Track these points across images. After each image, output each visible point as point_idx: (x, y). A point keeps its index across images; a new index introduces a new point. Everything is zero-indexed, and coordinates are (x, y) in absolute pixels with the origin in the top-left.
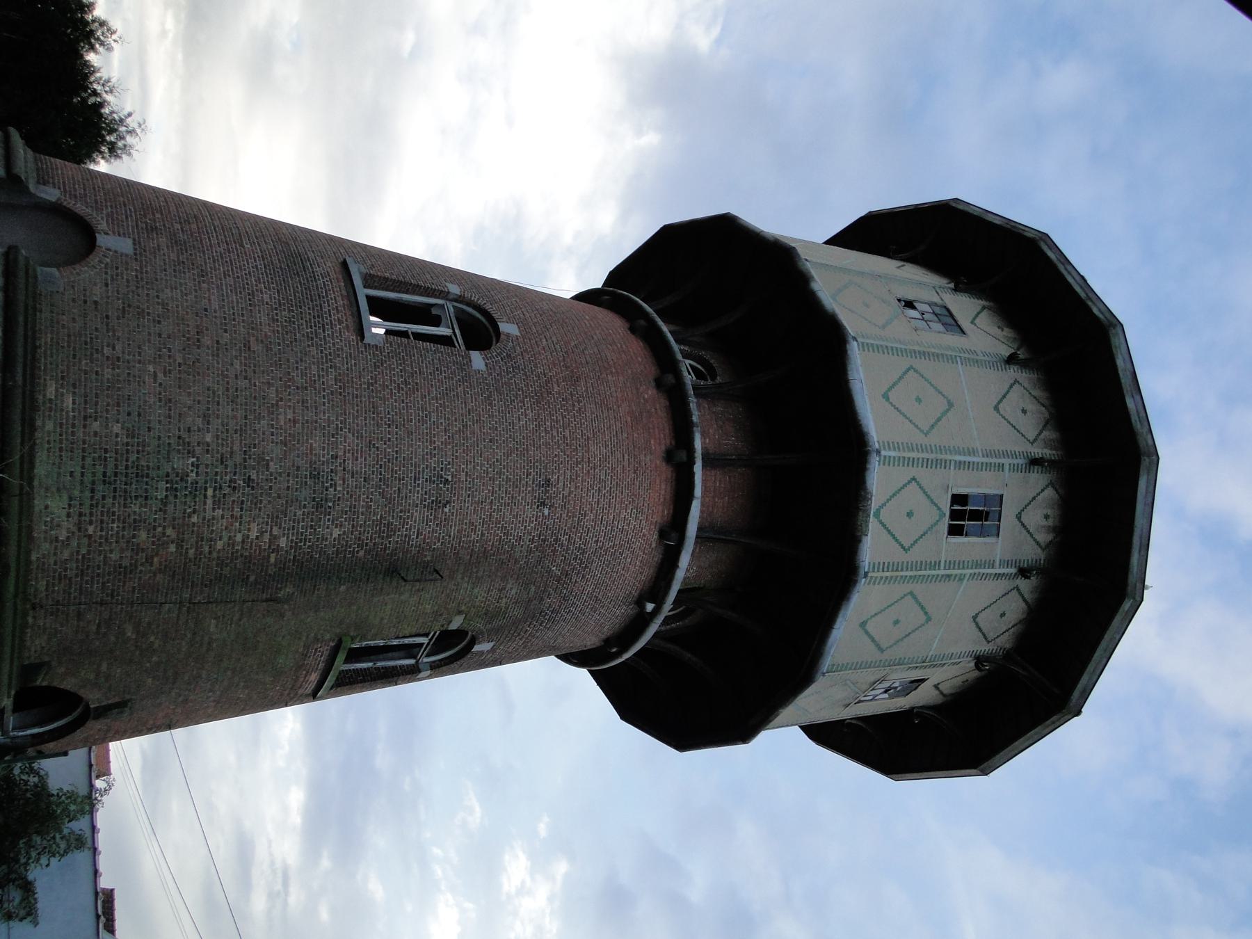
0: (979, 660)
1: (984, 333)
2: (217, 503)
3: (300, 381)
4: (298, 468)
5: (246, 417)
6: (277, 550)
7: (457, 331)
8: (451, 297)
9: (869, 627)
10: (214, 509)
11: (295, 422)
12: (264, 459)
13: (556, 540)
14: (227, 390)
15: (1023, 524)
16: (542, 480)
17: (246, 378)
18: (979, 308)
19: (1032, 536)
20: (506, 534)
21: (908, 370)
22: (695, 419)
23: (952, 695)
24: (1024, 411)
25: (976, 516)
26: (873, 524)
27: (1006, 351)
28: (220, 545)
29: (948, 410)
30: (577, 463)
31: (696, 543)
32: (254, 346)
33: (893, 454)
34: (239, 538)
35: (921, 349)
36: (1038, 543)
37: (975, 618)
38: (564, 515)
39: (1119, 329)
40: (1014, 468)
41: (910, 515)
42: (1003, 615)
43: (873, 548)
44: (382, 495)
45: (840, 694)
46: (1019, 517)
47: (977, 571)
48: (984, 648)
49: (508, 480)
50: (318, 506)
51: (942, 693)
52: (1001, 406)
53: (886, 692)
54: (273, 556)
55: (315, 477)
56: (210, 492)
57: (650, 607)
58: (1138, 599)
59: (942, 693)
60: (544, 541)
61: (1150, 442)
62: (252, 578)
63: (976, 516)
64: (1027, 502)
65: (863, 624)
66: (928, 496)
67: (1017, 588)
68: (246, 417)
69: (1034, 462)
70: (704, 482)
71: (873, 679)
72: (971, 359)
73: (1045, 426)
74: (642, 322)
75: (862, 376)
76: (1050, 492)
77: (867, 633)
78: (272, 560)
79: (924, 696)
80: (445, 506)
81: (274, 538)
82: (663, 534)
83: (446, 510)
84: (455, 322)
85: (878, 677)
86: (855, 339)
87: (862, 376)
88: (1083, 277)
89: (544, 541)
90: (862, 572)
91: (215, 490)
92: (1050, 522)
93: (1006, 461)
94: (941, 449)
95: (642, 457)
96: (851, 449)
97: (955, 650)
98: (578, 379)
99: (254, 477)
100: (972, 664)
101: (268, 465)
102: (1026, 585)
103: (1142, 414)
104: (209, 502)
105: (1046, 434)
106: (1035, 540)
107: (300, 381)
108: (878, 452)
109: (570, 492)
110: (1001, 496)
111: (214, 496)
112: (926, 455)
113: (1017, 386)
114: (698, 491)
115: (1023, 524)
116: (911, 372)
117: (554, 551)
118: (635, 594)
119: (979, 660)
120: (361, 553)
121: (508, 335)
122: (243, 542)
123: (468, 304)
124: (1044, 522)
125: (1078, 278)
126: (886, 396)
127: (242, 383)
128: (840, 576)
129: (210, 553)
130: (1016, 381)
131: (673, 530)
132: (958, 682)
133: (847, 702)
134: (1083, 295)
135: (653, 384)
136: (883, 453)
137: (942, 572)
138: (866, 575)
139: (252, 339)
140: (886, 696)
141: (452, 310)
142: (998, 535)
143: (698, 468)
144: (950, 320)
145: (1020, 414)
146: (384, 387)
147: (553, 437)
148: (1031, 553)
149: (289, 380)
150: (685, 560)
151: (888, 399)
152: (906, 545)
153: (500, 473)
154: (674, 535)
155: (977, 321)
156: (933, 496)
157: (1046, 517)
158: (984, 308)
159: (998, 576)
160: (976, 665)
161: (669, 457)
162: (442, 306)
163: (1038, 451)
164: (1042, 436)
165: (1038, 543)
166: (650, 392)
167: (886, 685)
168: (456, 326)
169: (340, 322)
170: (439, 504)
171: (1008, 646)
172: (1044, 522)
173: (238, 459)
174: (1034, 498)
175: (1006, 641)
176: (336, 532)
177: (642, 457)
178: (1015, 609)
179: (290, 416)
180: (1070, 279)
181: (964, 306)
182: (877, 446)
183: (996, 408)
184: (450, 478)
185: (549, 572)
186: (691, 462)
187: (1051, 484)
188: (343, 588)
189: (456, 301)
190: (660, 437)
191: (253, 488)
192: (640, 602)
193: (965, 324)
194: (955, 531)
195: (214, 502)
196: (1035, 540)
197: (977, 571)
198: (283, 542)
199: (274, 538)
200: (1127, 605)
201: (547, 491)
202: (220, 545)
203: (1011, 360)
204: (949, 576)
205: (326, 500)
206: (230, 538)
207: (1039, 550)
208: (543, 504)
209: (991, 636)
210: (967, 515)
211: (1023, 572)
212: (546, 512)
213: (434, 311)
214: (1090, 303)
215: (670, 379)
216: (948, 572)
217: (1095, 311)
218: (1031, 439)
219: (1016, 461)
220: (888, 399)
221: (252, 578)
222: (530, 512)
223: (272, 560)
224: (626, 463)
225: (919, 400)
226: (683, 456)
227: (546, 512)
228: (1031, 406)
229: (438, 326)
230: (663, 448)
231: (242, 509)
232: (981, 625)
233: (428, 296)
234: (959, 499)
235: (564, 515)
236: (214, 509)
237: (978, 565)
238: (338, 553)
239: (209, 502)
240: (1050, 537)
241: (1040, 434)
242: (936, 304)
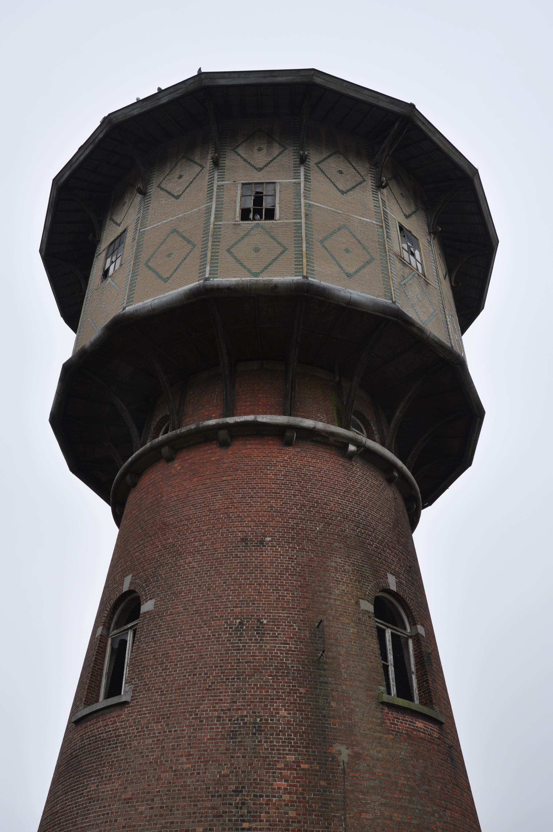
0: (380, 186)
1: (128, 218)
2: (255, 818)
3: (157, 753)
4: (227, 749)
5: (184, 798)
6: (298, 763)
7: (129, 626)
8: (105, 633)
9: (351, 270)
10: (260, 821)
11: (189, 755)
12: (219, 780)
13: (293, 529)
14: (161, 815)
15: (266, 166)
16: (241, 545)
17: (153, 800)
18: (111, 222)
19: (275, 158)
20: (287, 569)
21: (150, 268)
22: (193, 427)
23: (416, 205)
24: (180, 177)
25: (258, 199)
26: (264, 278)
27: (139, 197)
28: (292, 814)
29: (178, 232)
30: (229, 517)
31: (297, 416)
32: (129, 794)
33: (208, 269)
34: (286, 797)
35: (133, 259)
36: (280, 153)
37: (343, 192)
38: (271, 524)
39: (111, 117)
40: (221, 178)
41: (257, 250)
42: (341, 172)
43: (284, 276)
44: (251, 676)
45: (415, 290)
46: (260, 169)
47: (302, 195)
48: (370, 183)
49: (241, 573)
50: (260, 730)
51: (414, 213)
52: (176, 194)
53: (413, 254)
54: (303, 766)
55: (233, 734)
56: (246, 825)
57: (352, 448)
58: (313, 73)
59: (414, 213)
60: (293, 538)
61: (192, 81)
62: (323, 783)
63: (258, 199)
64: (248, 166)
65: (349, 276)
66: (242, 238)
67: (317, 164)
68: (184, 798)
69: (216, 164)
70: (240, 415)
71: (399, 265)
72: (141, 222)
73: (192, 161)
74: (128, 478)
75: (150, 300)
76: (241, 150)
77: (357, 272)
78: (306, 766)
79: (417, 226)
80: (262, 623)
81: (287, 766)
82: (288, 443)
83: (265, 622)
84: (122, 629)
85: (397, 262)
86: (124, 308)
87: (150, 300)
88: (80, 149)
89: (293, 538)
90: (305, 280)
91: (244, 821)
92: (264, 146)
93: (216, 184)
94: (206, 233)
95: (225, 466)
96: (206, 301)
97: (371, 204)
98: (164, 523)
99: (233, 787)
100: (385, 191)
101: (224, 776)
102: (314, 158)
103: (172, 90)
104: (254, 825)
105: (197, 159)
106: (278, 155)
107: (157, 753)
108: (206, 279)
109: (253, 521)
110: (243, 184)
111: (249, 821)
112: (210, 244)
113: (162, 186)
114: (250, 418)
115: (266, 166)
116: (150, 264)
117: (302, 530)
118: (342, 461)
119: (380, 186)
120: (302, 690)
121: (131, 583)
122: (290, 793)
123: (111, 619)
124: (264, 151)
125: (81, 153)
126: (166, 280)
127: (157, 803)
128: (306, 297)
129: (299, 822)
130: (159, 186)
131: (281, 435)
132: (402, 201)
133: (423, 283)
134: (91, 147)
135: (170, 464)
136: (207, 276)
137: (303, 221)
138: (306, 277)
139: (123, 796)
140: (417, 253)
141: (115, 632)
142: (274, 183)
143: (231, 420)
144: (118, 241)
145: (182, 180)
146: (165, 681)
147: (208, 539)
148: (288, 158)
149: (156, 762)
150: (308, 423)
151: (168, 278)
152: (281, 249)
153: (235, 579)
154: (288, 434)
155: (119, 222)
156: (242, 234)
157: (260, 150)
158: (112, 219)
159: (307, 179)
160: (384, 187)
161: (224, 445)
162: (113, 639)
163: (209, 164)
164: (198, 161)
165: (280, 153)
166: (176, 465)
167: (406, 255)
168: (126, 627)
169: (115, 722)
170: (260, 629)
171: (368, 166)
172: (264, 151)
173: (217, 802)
174: (245, 160)
175: (364, 168)
176: (283, 713)
177: (225, 466)
178: (334, 165)
179: (184, 759)
180: (82, 158)
181: (109, 235)
182: (201, 281)
183: (177, 197)
184: (238, 621)
185: (320, 532)
186: (227, 426)
187: (234, 150)
188: (333, 704)
189: (109, 629)
190: (211, 454)
191: (243, 787)
192: (350, 456)
193: (120, 229)
194: (270, 214)
195: (255, 821)
196: (278, 155)
197: (302, 195)
198: (291, 758)
199: (287, 766)
200: (318, 80)
201: (251, 540)
202: (292, 814)
203: (144, 193)
204: (306, 215)
205: (255, 723)
206: (286, 805)
207: (286, 151)
208: (262, 542)
209: (359, 179)
210: (259, 209)
211: (303, 160)
212: (268, 539)
213: (116, 646)
214: (97, 140)
215: (165, 451)
216: (303, 216)
217: (101, 136)
218: (200, 168)
219: (216, 178)
220: (168, 278)
221: (323, 783)
222: (268, 552)
223: (306, 766)
224: (229, 478)
225: (169, 255)
226: (223, 434)
227: (268, 539)
228: (177, 173)
229: (126, 641)
230: (218, 450)
231: (261, 796)
232: (349, 187)
233: (104, 652)
234: (245, 215)
235: (271, 524)
236: (262, 821)
237: (298, 195)
238: (301, 711)
239: (254, 825)
240: (276, 145)
241: (196, 163)
242: (107, 254)
